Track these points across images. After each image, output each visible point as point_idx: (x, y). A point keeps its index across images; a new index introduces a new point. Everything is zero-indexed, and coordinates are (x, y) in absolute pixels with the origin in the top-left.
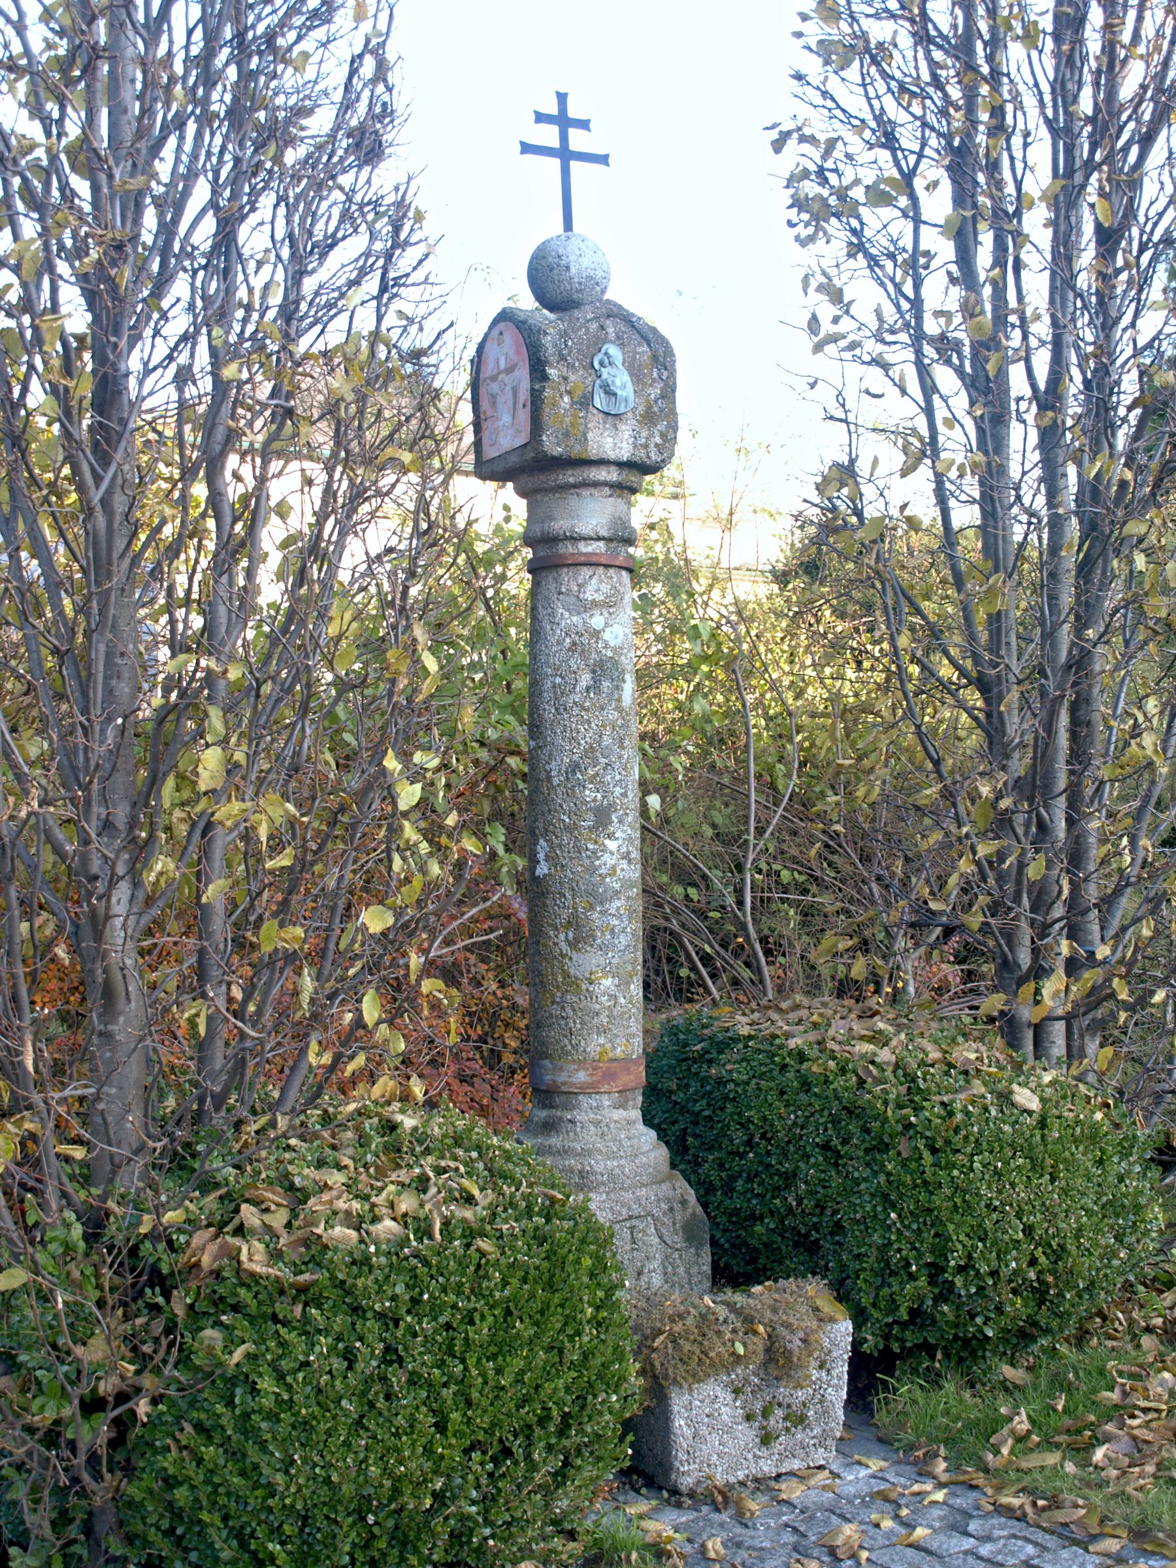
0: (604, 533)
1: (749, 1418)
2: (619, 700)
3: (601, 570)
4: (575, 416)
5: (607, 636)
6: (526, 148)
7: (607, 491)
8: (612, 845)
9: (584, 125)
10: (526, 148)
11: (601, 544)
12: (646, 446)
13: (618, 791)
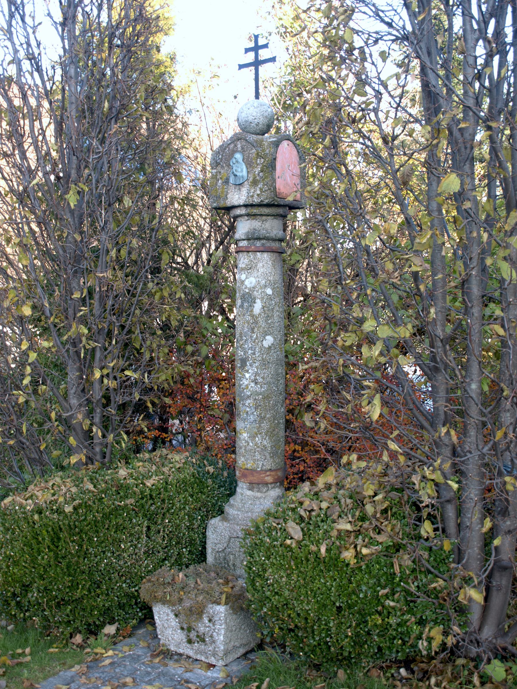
0: (243, 237)
1: (182, 629)
2: (252, 311)
3: (245, 253)
4: (223, 188)
5: (247, 283)
6: (241, 67)
7: (246, 218)
8: (247, 375)
9: (266, 46)
10: (241, 67)
11: (245, 242)
12: (252, 196)
13: (250, 352)
